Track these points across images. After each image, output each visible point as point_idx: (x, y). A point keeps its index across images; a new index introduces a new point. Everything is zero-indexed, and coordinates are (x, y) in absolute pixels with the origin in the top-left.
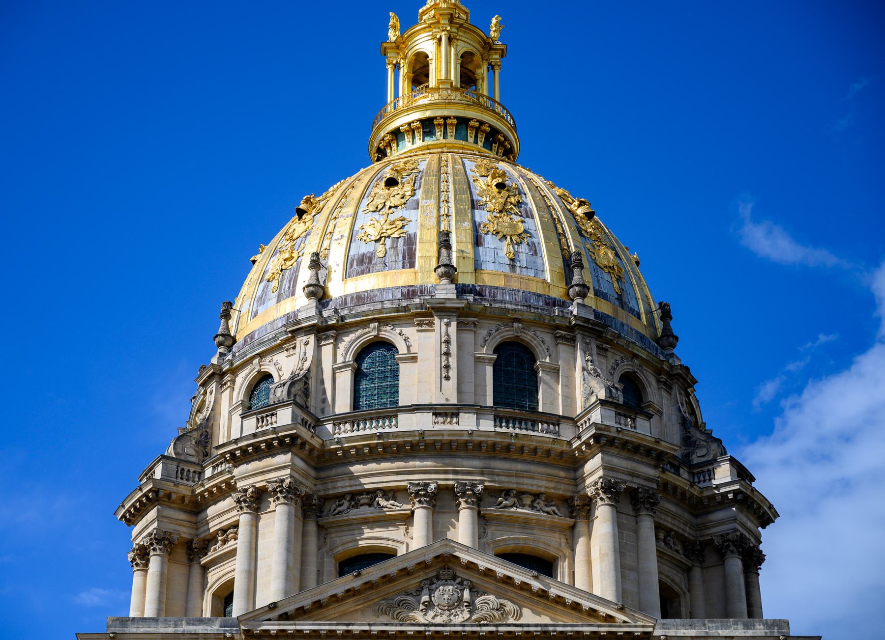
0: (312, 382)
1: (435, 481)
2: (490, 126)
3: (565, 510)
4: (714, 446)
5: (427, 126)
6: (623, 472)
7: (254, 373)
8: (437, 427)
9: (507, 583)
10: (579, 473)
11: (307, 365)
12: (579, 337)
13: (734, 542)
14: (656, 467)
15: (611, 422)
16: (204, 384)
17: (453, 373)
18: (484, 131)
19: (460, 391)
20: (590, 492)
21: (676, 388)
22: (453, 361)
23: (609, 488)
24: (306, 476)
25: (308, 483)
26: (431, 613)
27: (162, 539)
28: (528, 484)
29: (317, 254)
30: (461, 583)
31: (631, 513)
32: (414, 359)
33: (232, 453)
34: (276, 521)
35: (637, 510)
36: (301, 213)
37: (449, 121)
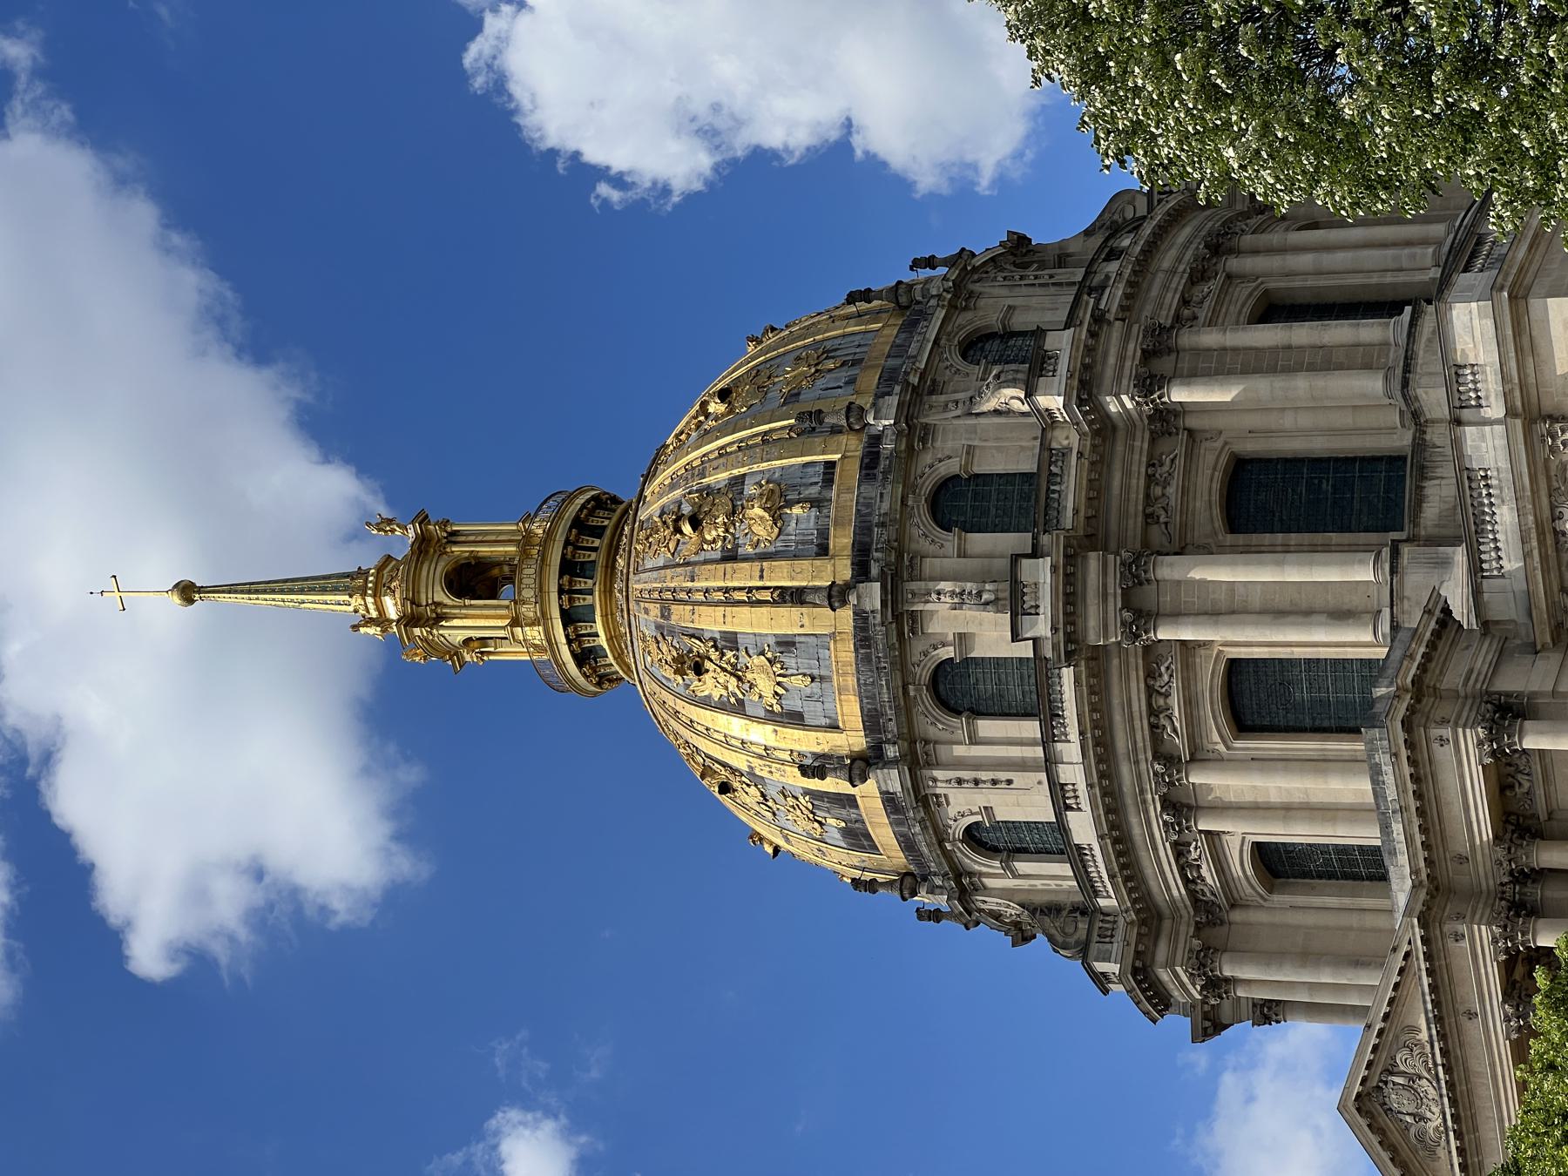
0: (1039, 899)
2: (561, 577)
6: (1106, 612)
8: (1085, 804)
14: (1085, 558)
17: (1003, 776)
19: (1022, 766)
22: (984, 775)
28: (1139, 704)
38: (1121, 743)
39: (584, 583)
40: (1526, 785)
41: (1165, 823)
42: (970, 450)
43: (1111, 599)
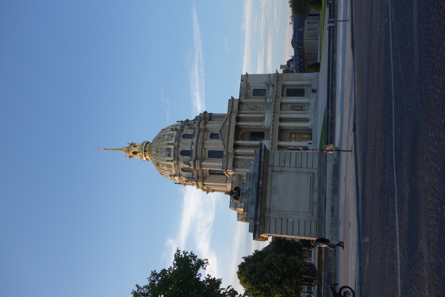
5: (145, 151)
27: (203, 181)
28: (202, 135)
38: (200, 137)
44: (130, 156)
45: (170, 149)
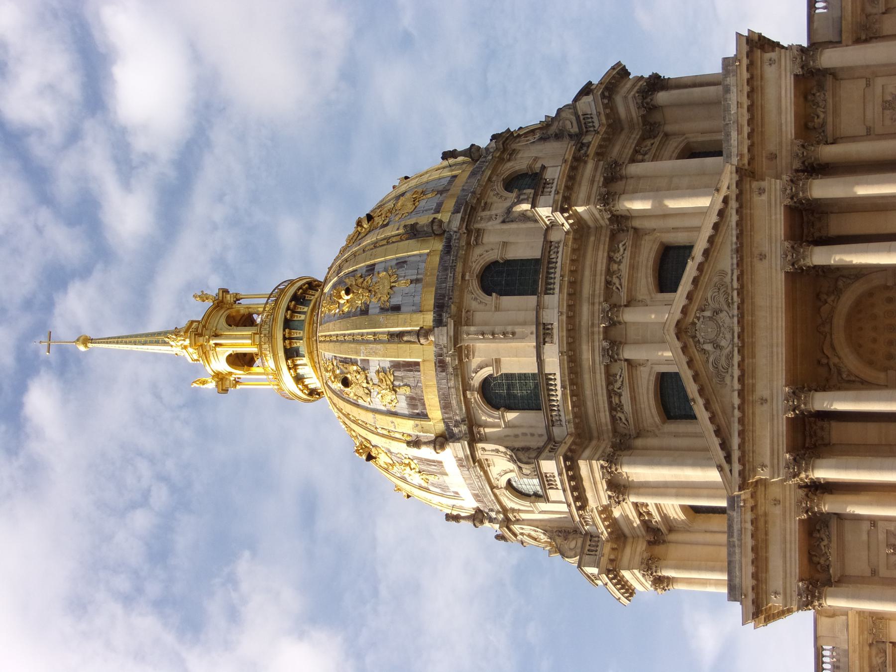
0: (518, 445)
1: (600, 342)
2: (291, 301)
3: (621, 235)
4: (563, 115)
5: (291, 354)
6: (591, 189)
7: (507, 493)
9: (698, 282)
10: (591, 223)
11: (502, 449)
12: (477, 226)
13: (644, 98)
14: (586, 162)
15: (550, 199)
16: (515, 535)
18: (295, 306)
19: (524, 324)
20: (607, 216)
21: (515, 146)
23: (607, 198)
24: (597, 448)
25: (603, 446)
26: (723, 343)
27: (649, 565)
28: (602, 266)
29: (409, 443)
30: (698, 318)
31: (624, 182)
32: (498, 362)
33: (579, 509)
34: (635, 472)
35: (622, 178)
36: (370, 458)
37: (287, 336)
38: (586, 290)
39: (301, 308)
40: (822, 116)
41: (603, 349)
42: (536, 159)
43: (596, 184)
44: (220, 378)
45: (413, 366)
